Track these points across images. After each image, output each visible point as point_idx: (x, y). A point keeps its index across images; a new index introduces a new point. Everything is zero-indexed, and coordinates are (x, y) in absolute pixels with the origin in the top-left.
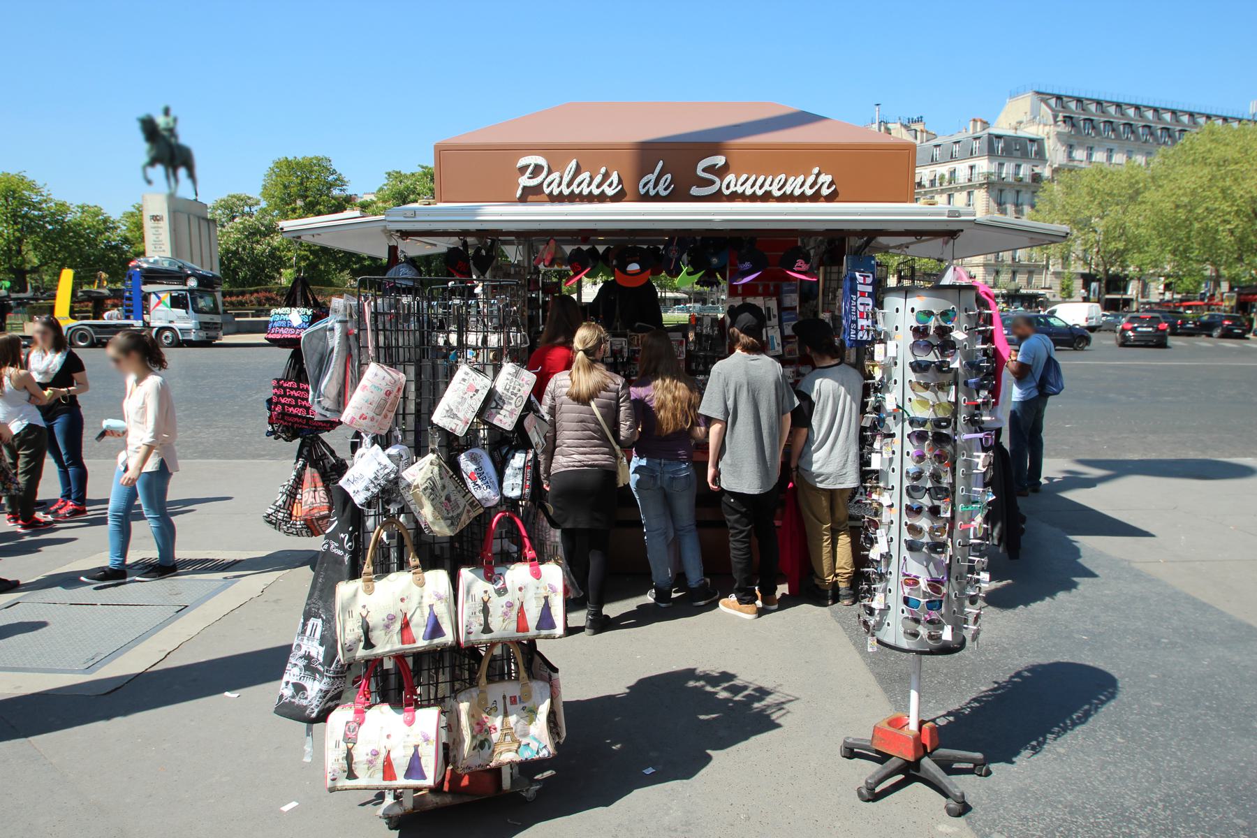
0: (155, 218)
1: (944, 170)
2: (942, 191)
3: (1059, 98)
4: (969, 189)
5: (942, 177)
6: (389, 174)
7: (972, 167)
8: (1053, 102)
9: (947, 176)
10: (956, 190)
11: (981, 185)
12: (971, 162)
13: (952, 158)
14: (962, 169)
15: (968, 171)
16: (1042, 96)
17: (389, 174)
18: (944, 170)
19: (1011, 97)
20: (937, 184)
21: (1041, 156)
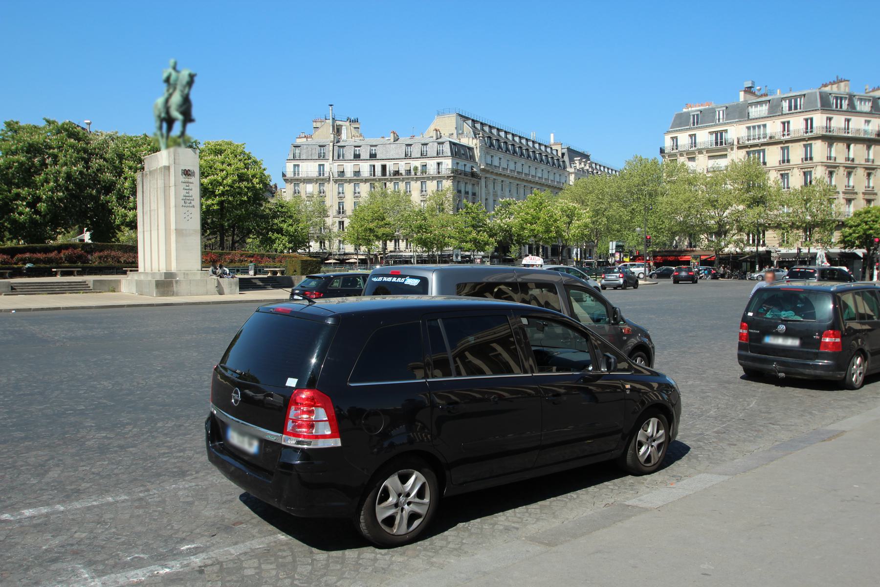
0: (187, 173)
1: (418, 163)
2: (417, 179)
3: (473, 121)
4: (439, 178)
5: (416, 168)
6: (8, 125)
7: (439, 164)
8: (470, 122)
9: (420, 168)
10: (428, 178)
11: (448, 177)
12: (439, 160)
13: (423, 155)
14: (432, 165)
15: (436, 166)
16: (465, 118)
17: (8, 125)
18: (418, 163)
19: (438, 114)
20: (413, 173)
21: (472, 158)
